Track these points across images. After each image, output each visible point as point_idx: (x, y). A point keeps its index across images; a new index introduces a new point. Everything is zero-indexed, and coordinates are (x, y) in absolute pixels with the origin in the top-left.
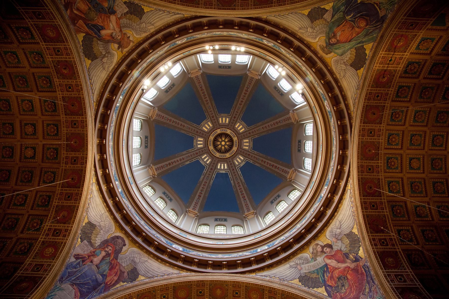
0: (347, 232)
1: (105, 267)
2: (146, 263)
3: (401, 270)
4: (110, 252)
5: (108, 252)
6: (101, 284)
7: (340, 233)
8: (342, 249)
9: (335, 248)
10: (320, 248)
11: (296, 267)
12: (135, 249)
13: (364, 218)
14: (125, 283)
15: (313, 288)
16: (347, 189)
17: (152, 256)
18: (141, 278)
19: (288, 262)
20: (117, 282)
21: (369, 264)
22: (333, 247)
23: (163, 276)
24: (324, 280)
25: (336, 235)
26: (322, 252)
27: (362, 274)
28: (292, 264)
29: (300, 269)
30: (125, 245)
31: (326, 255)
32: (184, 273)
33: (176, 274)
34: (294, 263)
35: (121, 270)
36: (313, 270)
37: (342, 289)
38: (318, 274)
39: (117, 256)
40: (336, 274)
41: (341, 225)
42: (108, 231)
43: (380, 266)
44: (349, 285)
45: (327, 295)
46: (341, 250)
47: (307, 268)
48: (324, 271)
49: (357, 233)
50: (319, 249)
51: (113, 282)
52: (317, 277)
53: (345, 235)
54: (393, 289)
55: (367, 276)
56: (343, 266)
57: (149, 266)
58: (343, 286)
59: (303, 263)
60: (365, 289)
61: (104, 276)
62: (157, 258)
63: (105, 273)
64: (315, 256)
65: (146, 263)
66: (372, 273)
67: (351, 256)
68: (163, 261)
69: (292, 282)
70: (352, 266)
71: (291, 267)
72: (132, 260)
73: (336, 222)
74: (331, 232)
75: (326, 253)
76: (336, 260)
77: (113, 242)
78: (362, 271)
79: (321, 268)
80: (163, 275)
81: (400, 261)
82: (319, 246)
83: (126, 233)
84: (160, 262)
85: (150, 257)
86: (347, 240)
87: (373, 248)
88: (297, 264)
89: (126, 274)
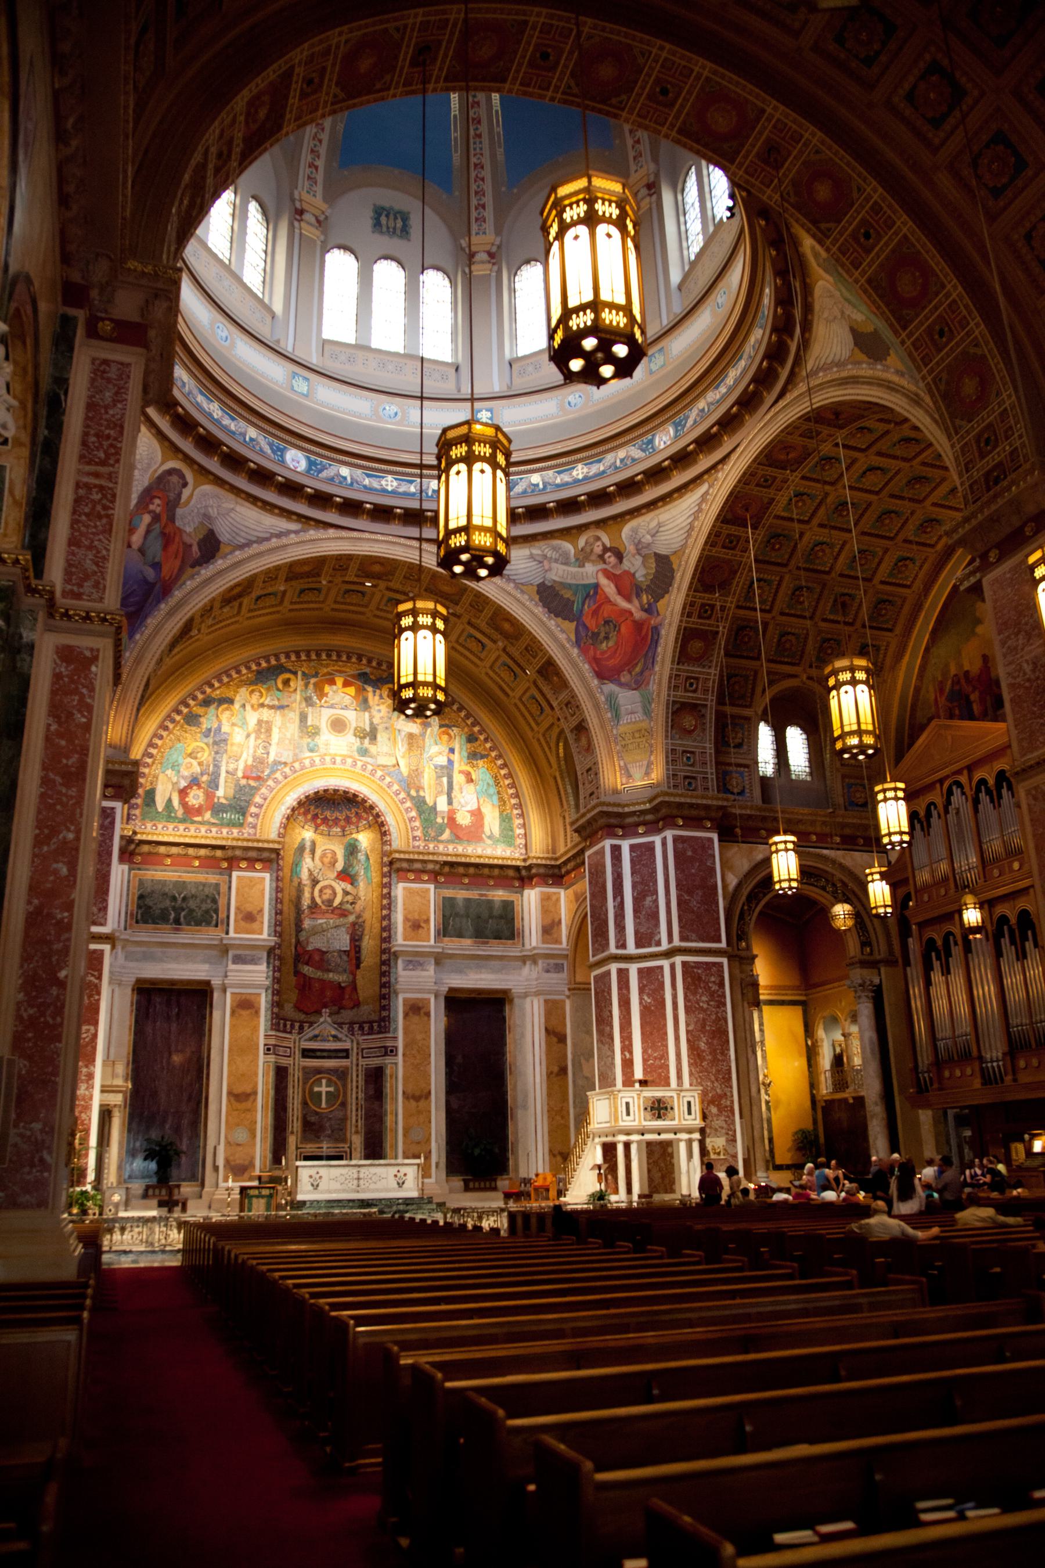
0: (663, 551)
1: (155, 548)
2: (232, 515)
3: (704, 667)
4: (158, 510)
5: (153, 512)
6: (156, 583)
7: (649, 544)
8: (637, 575)
9: (626, 565)
10: (601, 548)
11: (541, 562)
12: (207, 488)
13: (699, 561)
14: (197, 569)
15: (557, 616)
16: (706, 477)
17: (243, 495)
18: (224, 549)
19: (528, 545)
20: (181, 570)
21: (663, 632)
22: (624, 560)
23: (267, 539)
24: (581, 611)
25: (640, 542)
26: (601, 557)
27: (644, 639)
28: (536, 551)
29: (547, 567)
30: (185, 485)
31: (604, 566)
32: (312, 533)
33: (296, 532)
34: (539, 552)
35: (184, 544)
36: (569, 581)
37: (602, 643)
38: (575, 594)
39: (174, 515)
40: (606, 611)
41: (657, 532)
42: (149, 465)
43: (674, 656)
44: (617, 643)
45: (574, 639)
46: (633, 575)
47: (560, 573)
48: (588, 595)
49: (675, 567)
50: (598, 549)
51: (176, 571)
52: (572, 599)
53: (656, 554)
54: (668, 704)
55: (650, 647)
56: (624, 604)
57: (238, 520)
58: (607, 638)
59: (556, 561)
60: (637, 664)
61: (156, 566)
62: (254, 500)
63: (156, 560)
64: (583, 557)
65: (232, 515)
66: (660, 649)
67: (645, 597)
68: (267, 507)
69: (524, 588)
70: (638, 615)
71: (532, 557)
72: (205, 515)
73: (652, 519)
74: (635, 531)
75: (605, 562)
76: (617, 587)
77: (161, 486)
78: (647, 635)
79: (585, 586)
80: (268, 535)
81: (712, 655)
82: (599, 543)
83: (187, 459)
84: (261, 508)
85: (240, 500)
86: (654, 565)
87: (681, 621)
88: (545, 557)
89: (195, 548)
